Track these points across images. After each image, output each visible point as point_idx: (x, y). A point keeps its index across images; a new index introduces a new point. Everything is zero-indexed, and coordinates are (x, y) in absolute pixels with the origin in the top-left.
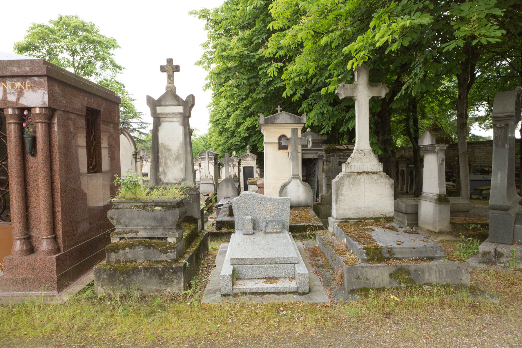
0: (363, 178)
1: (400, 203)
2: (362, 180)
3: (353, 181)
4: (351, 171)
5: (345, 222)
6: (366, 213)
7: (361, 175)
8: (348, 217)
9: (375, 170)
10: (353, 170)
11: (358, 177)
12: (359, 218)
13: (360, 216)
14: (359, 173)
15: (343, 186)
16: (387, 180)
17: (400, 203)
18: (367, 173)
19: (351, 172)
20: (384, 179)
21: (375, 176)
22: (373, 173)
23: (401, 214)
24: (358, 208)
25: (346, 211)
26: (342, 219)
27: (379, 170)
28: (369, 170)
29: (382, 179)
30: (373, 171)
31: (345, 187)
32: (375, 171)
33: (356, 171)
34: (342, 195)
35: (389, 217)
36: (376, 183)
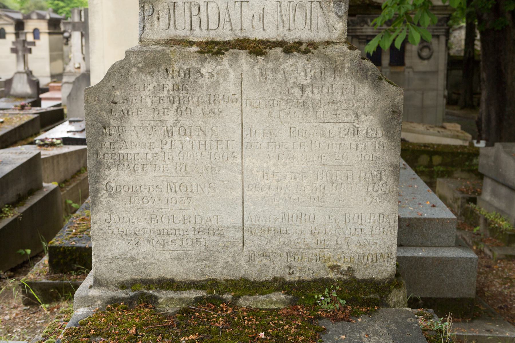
0: (232, 75)
1: (503, 156)
2: (230, 85)
3: (177, 88)
4: (172, 33)
5: (129, 303)
6: (251, 258)
7: (225, 60)
8: (154, 273)
9: (300, 32)
10: (181, 32)
11: (208, 68)
12: (213, 284)
13: (219, 272)
14: (214, 49)
15: (124, 114)
16: (365, 91)
17: (503, 156)
18: (257, 48)
19: (171, 42)
20: (350, 83)
21: (297, 67)
22: (290, 48)
23: (503, 191)
24: (208, 231)
25: (145, 247)
26: (123, 286)
27: (324, 35)
28: (270, 34)
29: (338, 82)
30: (291, 37)
31: (134, 121)
32: (305, 35)
33: (200, 35)
34: (120, 161)
35: (372, 284)
36: (304, 105)
